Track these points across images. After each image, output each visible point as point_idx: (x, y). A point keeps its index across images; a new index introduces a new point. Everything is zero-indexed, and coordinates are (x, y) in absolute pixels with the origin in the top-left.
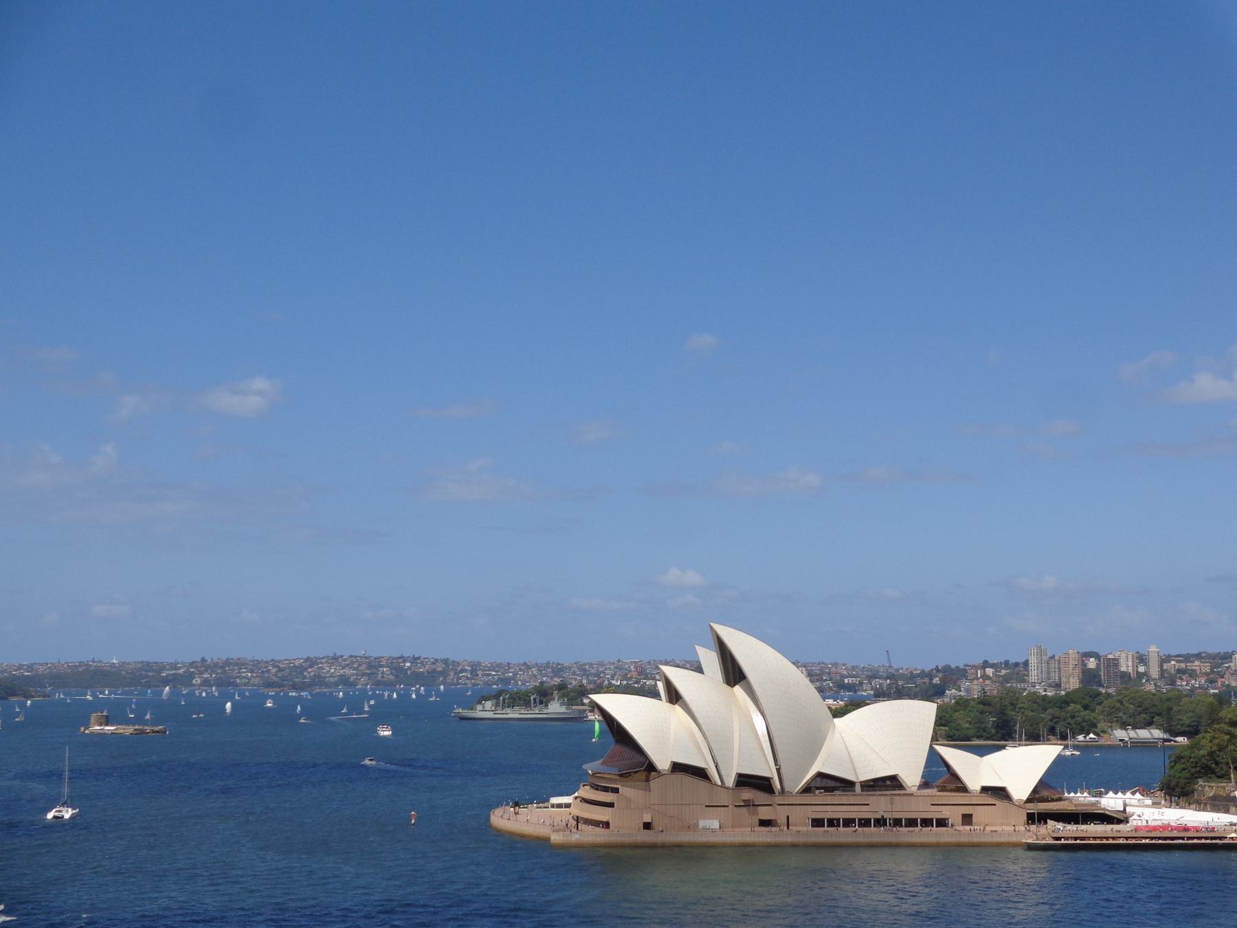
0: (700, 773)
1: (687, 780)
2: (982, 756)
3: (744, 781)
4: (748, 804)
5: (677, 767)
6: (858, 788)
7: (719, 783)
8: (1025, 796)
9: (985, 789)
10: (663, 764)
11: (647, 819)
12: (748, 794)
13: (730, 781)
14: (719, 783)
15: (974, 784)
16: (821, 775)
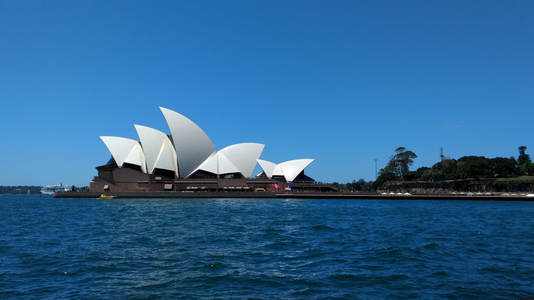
0: (137, 168)
1: (130, 170)
2: (277, 163)
3: (158, 172)
4: (158, 182)
5: (126, 165)
6: (219, 177)
7: (146, 172)
8: (292, 180)
9: (273, 176)
10: (120, 164)
11: (106, 187)
12: (158, 178)
13: (151, 172)
14: (146, 172)
15: (269, 175)
16: (200, 171)
